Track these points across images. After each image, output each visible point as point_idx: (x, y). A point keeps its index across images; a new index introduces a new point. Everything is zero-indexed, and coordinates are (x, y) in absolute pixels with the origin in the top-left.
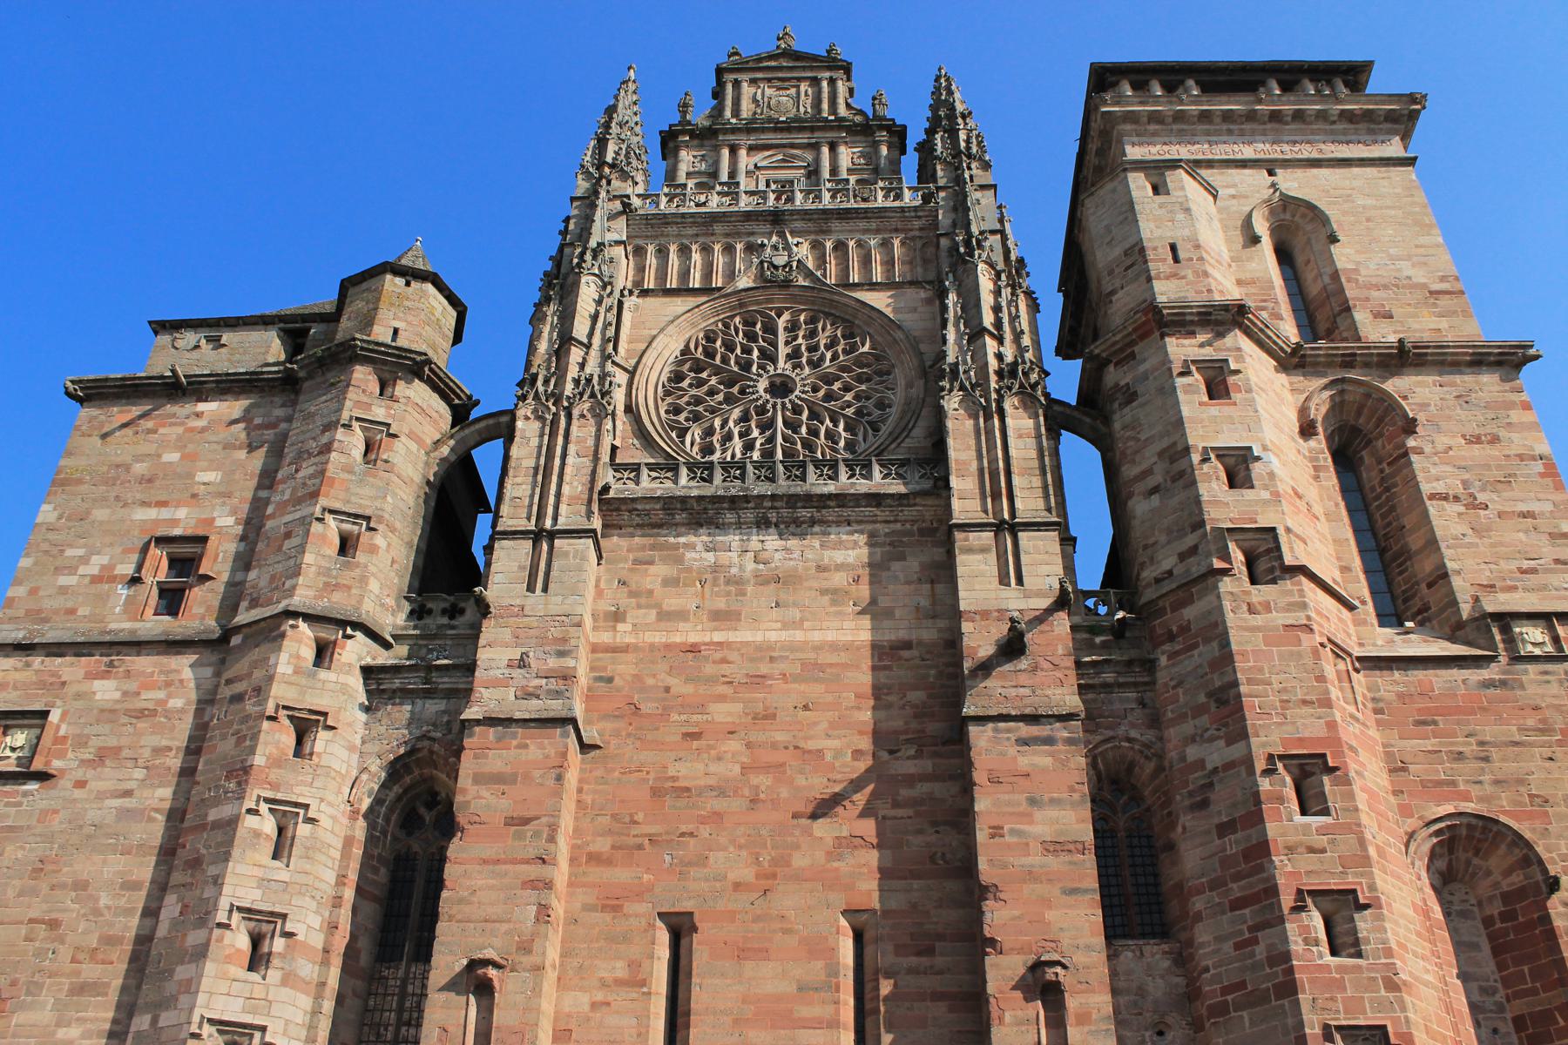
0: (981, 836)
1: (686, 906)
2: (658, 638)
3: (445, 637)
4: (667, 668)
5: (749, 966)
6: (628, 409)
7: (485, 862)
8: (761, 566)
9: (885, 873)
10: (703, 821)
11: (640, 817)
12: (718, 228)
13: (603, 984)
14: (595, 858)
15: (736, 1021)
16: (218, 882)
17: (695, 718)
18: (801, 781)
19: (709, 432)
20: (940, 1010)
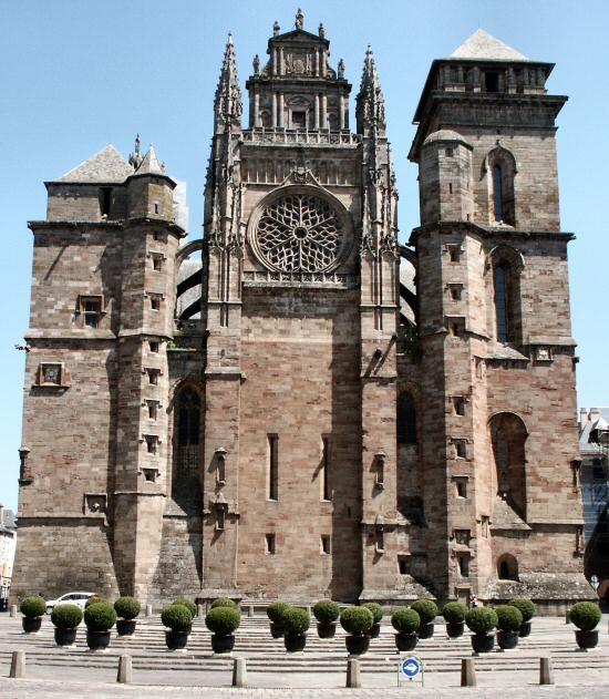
0: (363, 415)
1: (276, 431)
2: (263, 340)
6: (246, 242)
7: (217, 420)
9: (333, 423)
10: (280, 404)
14: (247, 415)
16: (137, 427)
19: (274, 252)
20: (349, 464)
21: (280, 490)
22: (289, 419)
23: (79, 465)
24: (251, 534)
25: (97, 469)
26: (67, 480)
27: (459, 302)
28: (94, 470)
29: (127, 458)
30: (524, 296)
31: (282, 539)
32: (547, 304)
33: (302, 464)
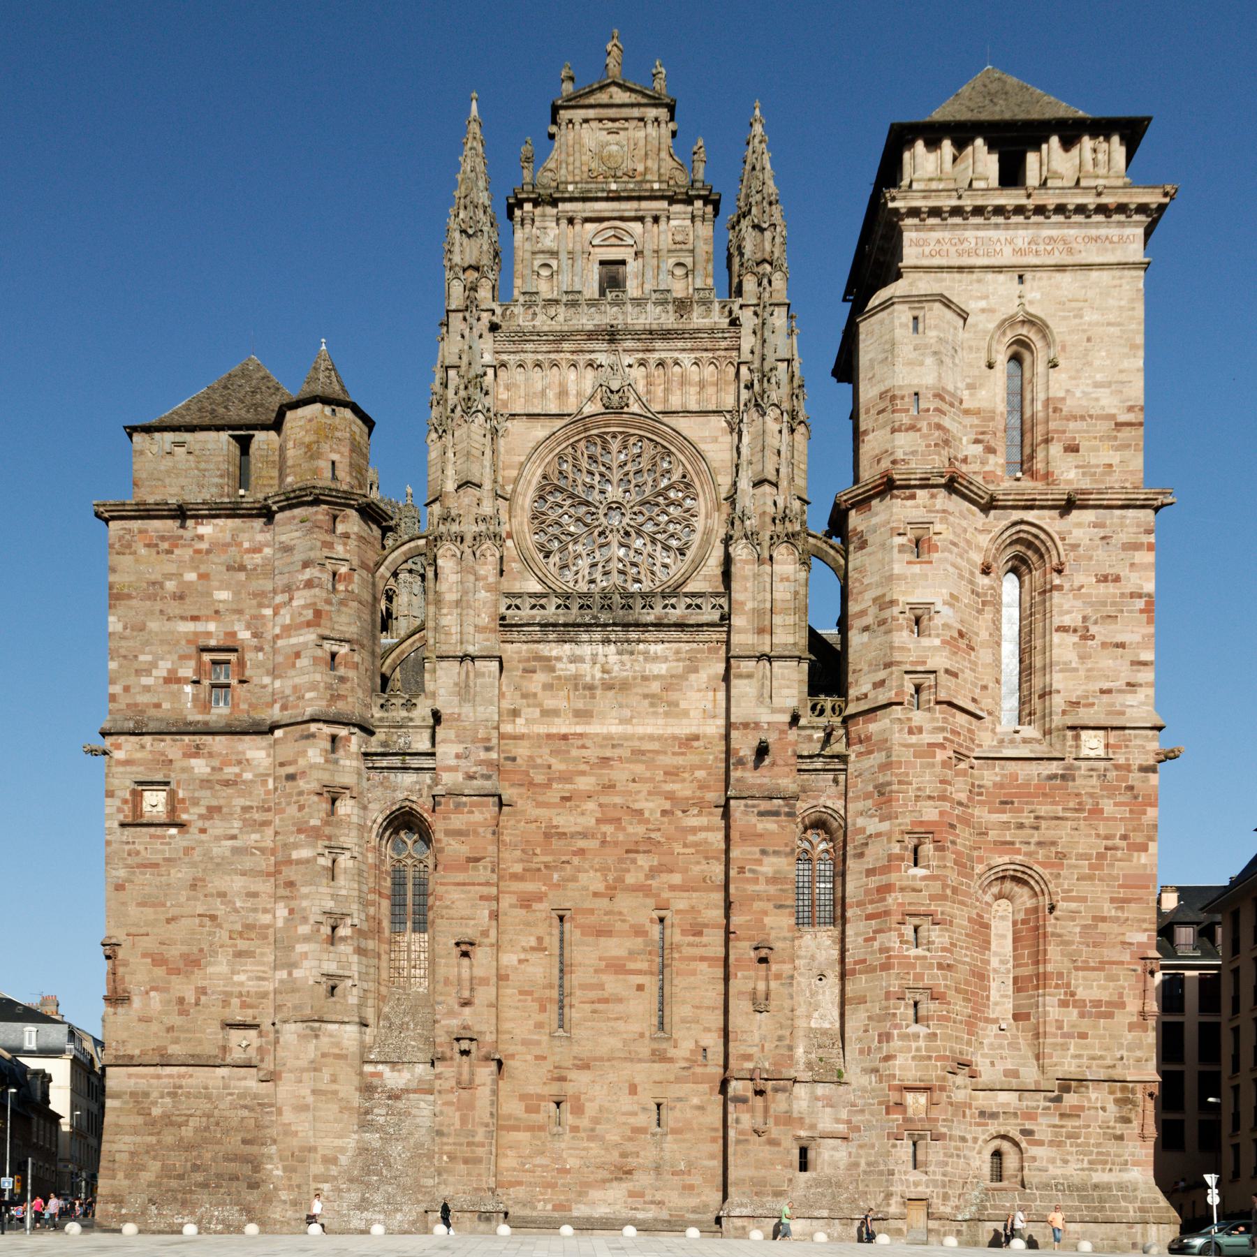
1: (568, 905)
2: (542, 729)
3: (407, 727)
4: (548, 751)
5: (602, 939)
8: (606, 676)
10: (575, 853)
11: (538, 851)
12: (566, 346)
13: (524, 950)
15: (596, 971)
17: (568, 786)
18: (630, 829)
20: (703, 966)
21: (574, 1014)
22: (592, 881)
23: (210, 970)
24: (523, 1097)
25: (241, 978)
26: (190, 997)
27: (925, 642)
28: (236, 978)
29: (294, 957)
30: (1062, 629)
31: (578, 1110)
32: (1104, 645)
33: (617, 967)
